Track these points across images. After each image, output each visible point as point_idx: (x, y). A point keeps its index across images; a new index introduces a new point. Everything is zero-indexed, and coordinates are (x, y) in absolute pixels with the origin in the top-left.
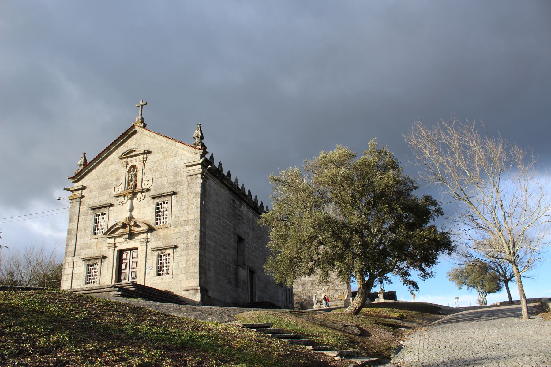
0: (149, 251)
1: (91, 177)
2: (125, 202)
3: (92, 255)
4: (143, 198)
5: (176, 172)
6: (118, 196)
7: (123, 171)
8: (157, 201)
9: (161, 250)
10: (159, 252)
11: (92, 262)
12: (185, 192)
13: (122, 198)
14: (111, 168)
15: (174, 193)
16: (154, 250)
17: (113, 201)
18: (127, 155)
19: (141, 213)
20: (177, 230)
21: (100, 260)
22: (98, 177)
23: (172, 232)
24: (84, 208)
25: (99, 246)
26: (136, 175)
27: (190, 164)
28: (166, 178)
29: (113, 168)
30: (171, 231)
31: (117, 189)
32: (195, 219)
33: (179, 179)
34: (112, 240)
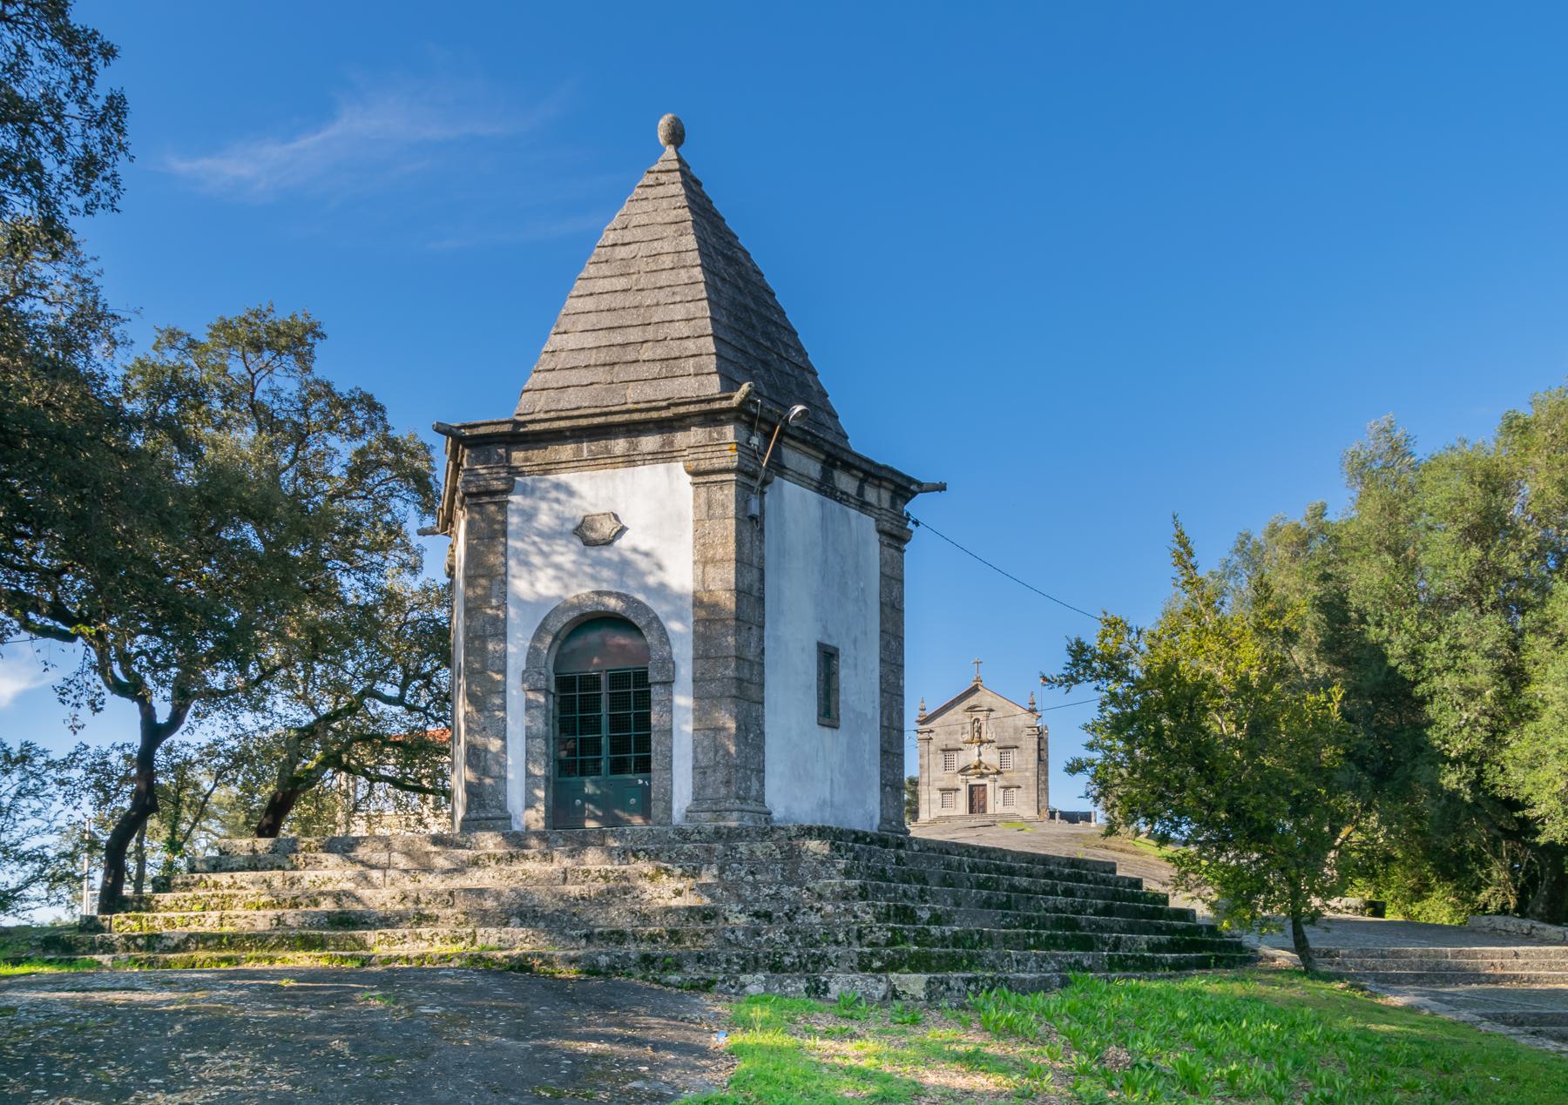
5: (1016, 729)
9: (1006, 788)
18: (972, 709)
24: (932, 748)
29: (957, 715)
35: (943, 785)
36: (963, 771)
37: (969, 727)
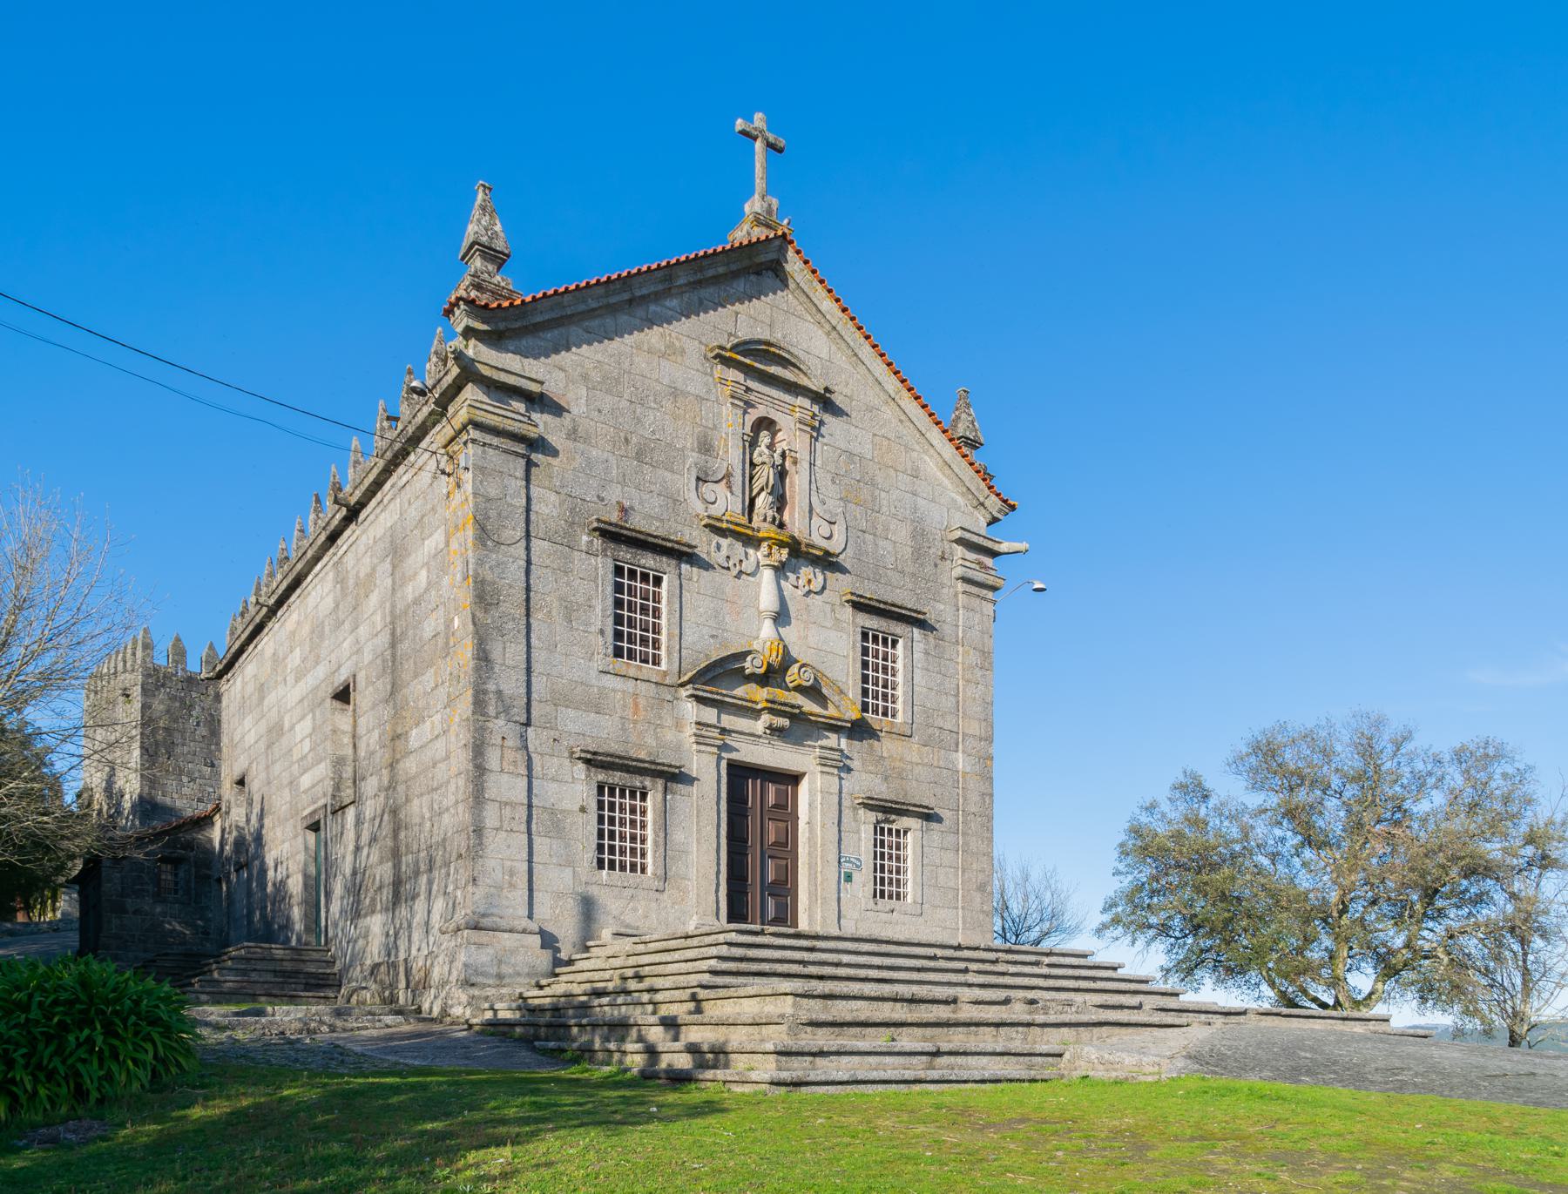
0: (846, 803)
2: (748, 566)
3: (614, 747)
4: (816, 586)
5: (919, 534)
6: (723, 533)
7: (730, 425)
9: (887, 810)
10: (880, 816)
11: (624, 777)
13: (738, 545)
14: (669, 372)
15: (922, 624)
16: (871, 805)
17: (705, 545)
21: (660, 783)
22: (610, 384)
23: (916, 759)
24: (547, 506)
26: (782, 474)
27: (975, 539)
30: (912, 751)
31: (706, 489)
34: (710, 715)
35: (606, 734)
36: (718, 676)
37: (731, 455)
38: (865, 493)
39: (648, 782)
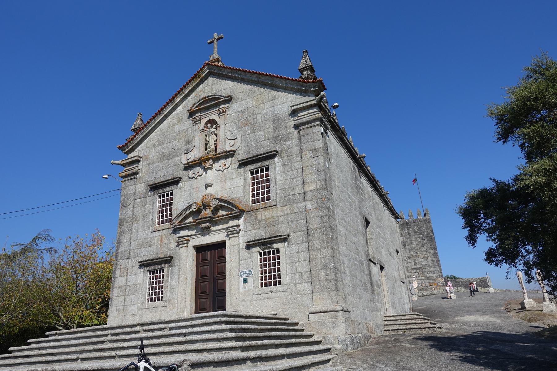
1: (150, 144)
3: (154, 257)
5: (277, 120)
8: (251, 167)
12: (295, 150)
19: (227, 187)
20: (287, 210)
22: (160, 142)
23: (279, 213)
25: (165, 241)
28: (262, 133)
30: (277, 212)
32: (317, 190)
33: (283, 131)
38: (250, 120)
39: (163, 266)
